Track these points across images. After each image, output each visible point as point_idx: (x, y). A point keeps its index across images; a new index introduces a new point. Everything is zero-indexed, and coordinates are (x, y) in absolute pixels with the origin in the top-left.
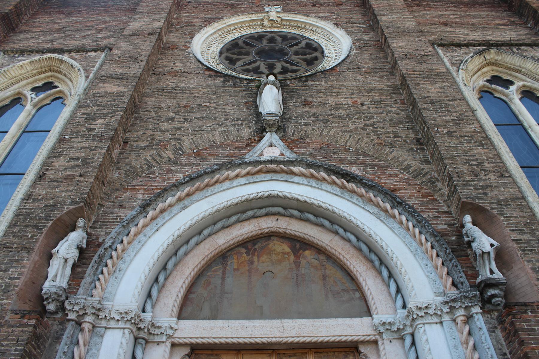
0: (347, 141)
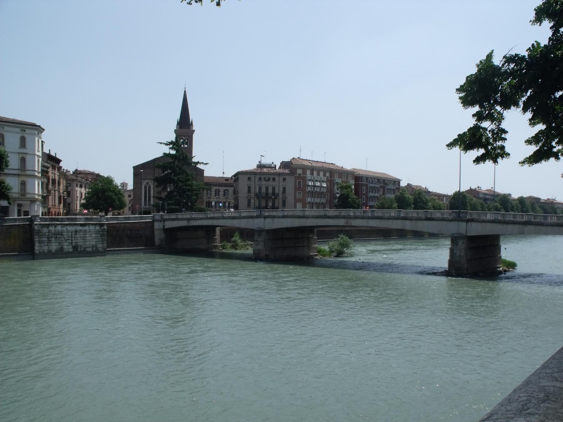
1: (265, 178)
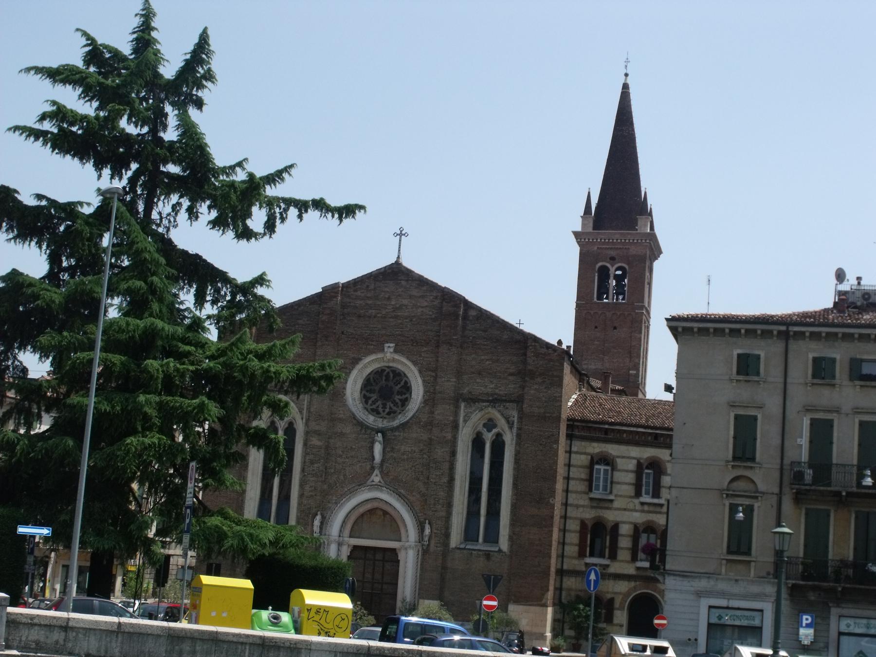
1: (855, 365)
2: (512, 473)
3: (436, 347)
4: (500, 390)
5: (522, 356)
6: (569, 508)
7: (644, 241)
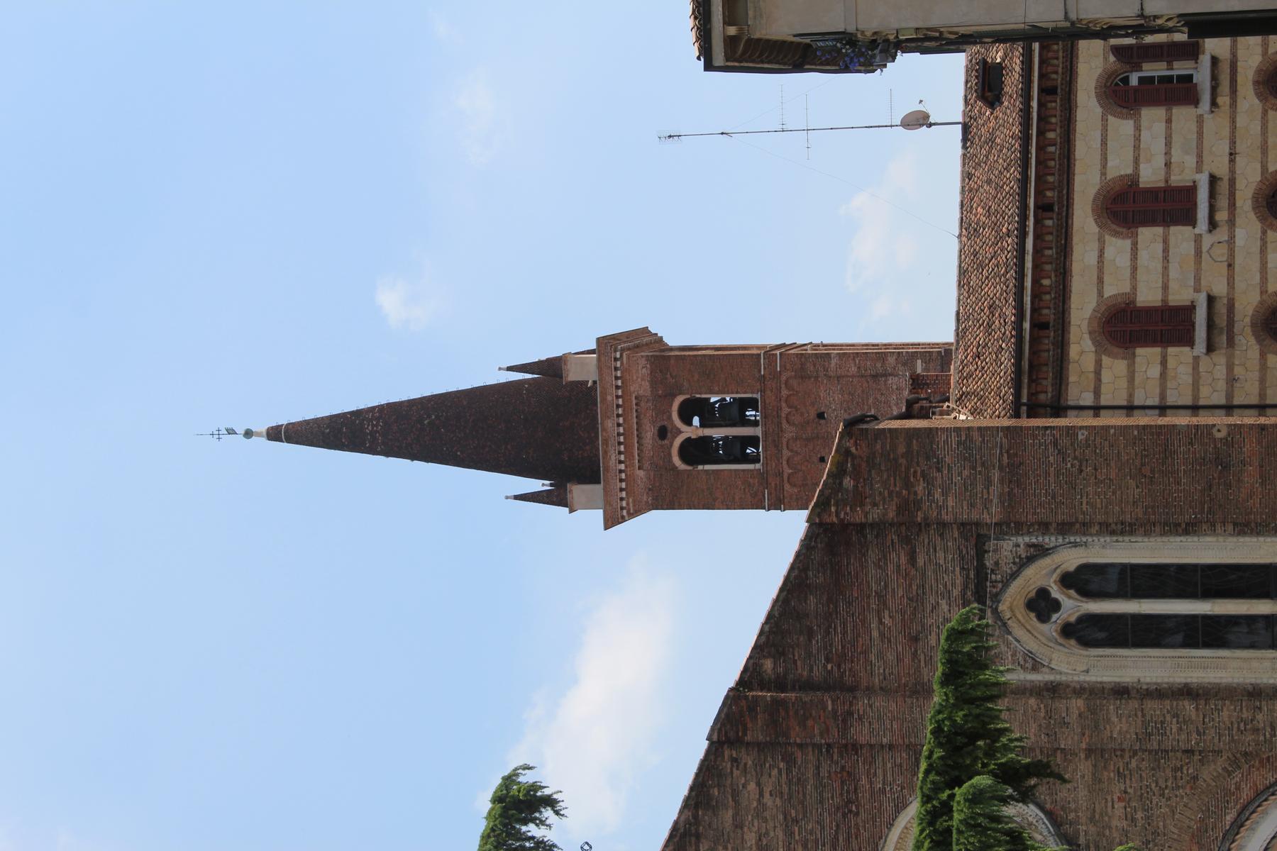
0: (1189, 818)
2: (1159, 539)
3: (857, 753)
4: (953, 585)
5: (865, 537)
6: (1236, 402)
7: (618, 364)
